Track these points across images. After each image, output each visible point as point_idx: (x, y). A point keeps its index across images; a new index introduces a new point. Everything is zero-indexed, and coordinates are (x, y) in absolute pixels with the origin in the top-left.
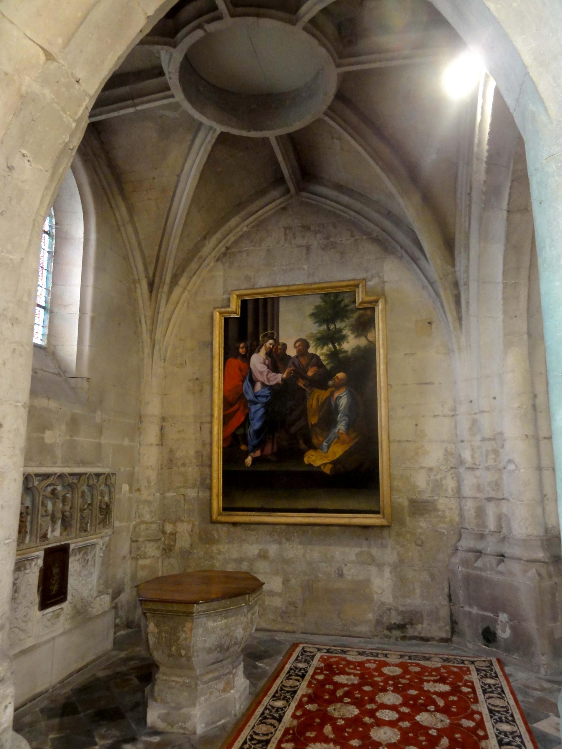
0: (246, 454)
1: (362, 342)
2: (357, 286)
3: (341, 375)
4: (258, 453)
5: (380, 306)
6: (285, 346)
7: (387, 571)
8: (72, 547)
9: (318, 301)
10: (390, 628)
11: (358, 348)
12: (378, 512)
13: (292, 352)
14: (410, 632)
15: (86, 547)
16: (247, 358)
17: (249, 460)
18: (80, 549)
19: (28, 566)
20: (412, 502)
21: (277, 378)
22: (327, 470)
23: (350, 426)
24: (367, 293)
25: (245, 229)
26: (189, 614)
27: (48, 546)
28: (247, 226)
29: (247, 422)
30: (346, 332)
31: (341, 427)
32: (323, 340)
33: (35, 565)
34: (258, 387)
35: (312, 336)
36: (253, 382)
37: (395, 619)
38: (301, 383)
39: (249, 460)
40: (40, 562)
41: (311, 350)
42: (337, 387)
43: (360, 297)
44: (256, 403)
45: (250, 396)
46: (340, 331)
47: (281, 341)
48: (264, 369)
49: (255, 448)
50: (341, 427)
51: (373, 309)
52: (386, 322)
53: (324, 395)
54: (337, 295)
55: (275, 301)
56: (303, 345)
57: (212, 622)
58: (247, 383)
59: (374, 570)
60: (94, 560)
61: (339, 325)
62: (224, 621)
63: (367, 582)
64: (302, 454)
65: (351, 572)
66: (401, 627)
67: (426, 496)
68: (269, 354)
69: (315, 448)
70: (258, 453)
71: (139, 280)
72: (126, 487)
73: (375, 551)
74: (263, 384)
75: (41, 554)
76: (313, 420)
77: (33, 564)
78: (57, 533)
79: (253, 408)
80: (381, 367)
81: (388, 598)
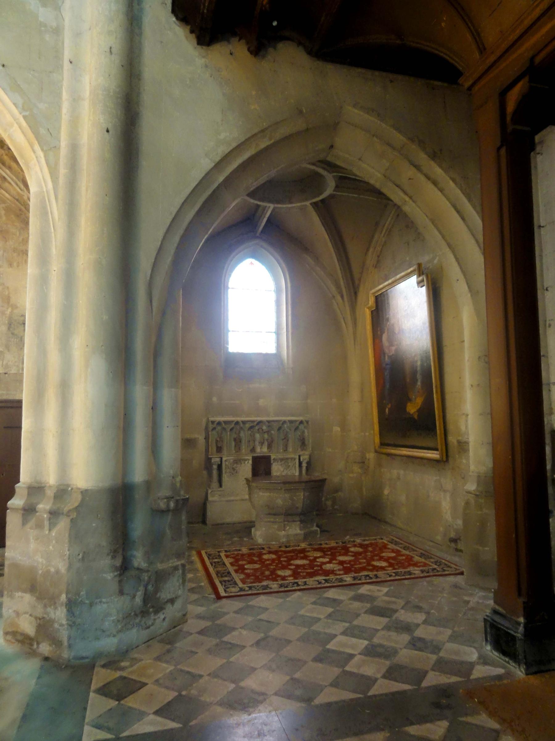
8: (273, 457)
15: (287, 459)
18: (282, 460)
19: (243, 463)
25: (384, 240)
27: (254, 455)
28: (384, 236)
33: (248, 463)
40: (250, 462)
57: (262, 493)
60: (295, 467)
62: (268, 494)
71: (334, 297)
72: (337, 429)
75: (250, 458)
77: (246, 462)
78: (265, 449)
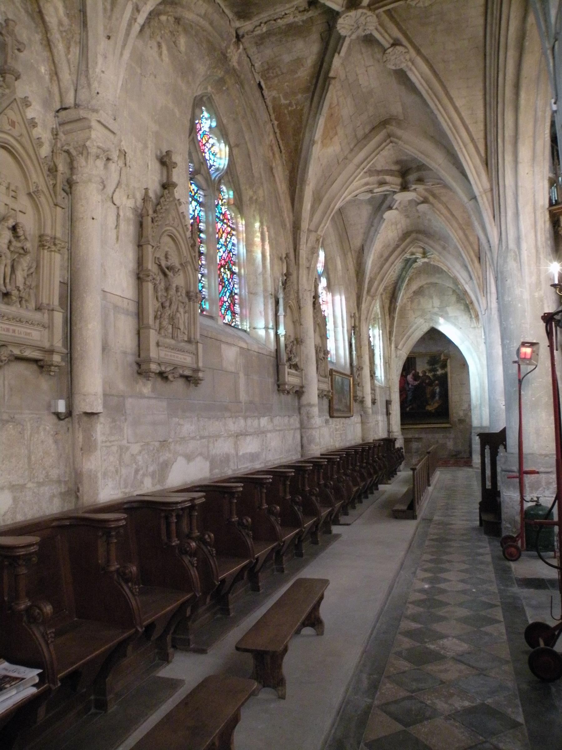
0: (407, 407)
1: (443, 372)
2: (441, 354)
3: (437, 382)
4: (411, 407)
5: (449, 361)
6: (418, 373)
7: (451, 440)
9: (429, 358)
10: (452, 456)
11: (442, 374)
12: (448, 423)
13: (421, 375)
14: (458, 456)
16: (406, 377)
17: (408, 409)
20: (459, 420)
21: (416, 383)
22: (433, 411)
23: (440, 397)
24: (444, 356)
26: (411, 441)
29: (406, 397)
30: (438, 368)
31: (437, 398)
32: (430, 371)
34: (410, 386)
35: (427, 369)
36: (408, 384)
37: (454, 453)
38: (424, 384)
39: (408, 409)
41: (427, 374)
42: (436, 386)
43: (442, 357)
44: (409, 391)
45: (407, 389)
46: (435, 368)
47: (417, 371)
48: (412, 380)
49: (410, 405)
50: (437, 398)
51: (446, 361)
52: (450, 365)
53: (432, 388)
54: (435, 356)
55: (415, 358)
56: (424, 372)
58: (406, 385)
59: (448, 440)
61: (436, 366)
63: (446, 444)
64: (425, 406)
65: (441, 441)
66: (456, 455)
67: (463, 418)
68: (413, 375)
69: (429, 405)
70: (411, 407)
73: (448, 435)
74: (412, 385)
76: (428, 396)
79: (409, 392)
80: (449, 380)
81: (452, 448)
